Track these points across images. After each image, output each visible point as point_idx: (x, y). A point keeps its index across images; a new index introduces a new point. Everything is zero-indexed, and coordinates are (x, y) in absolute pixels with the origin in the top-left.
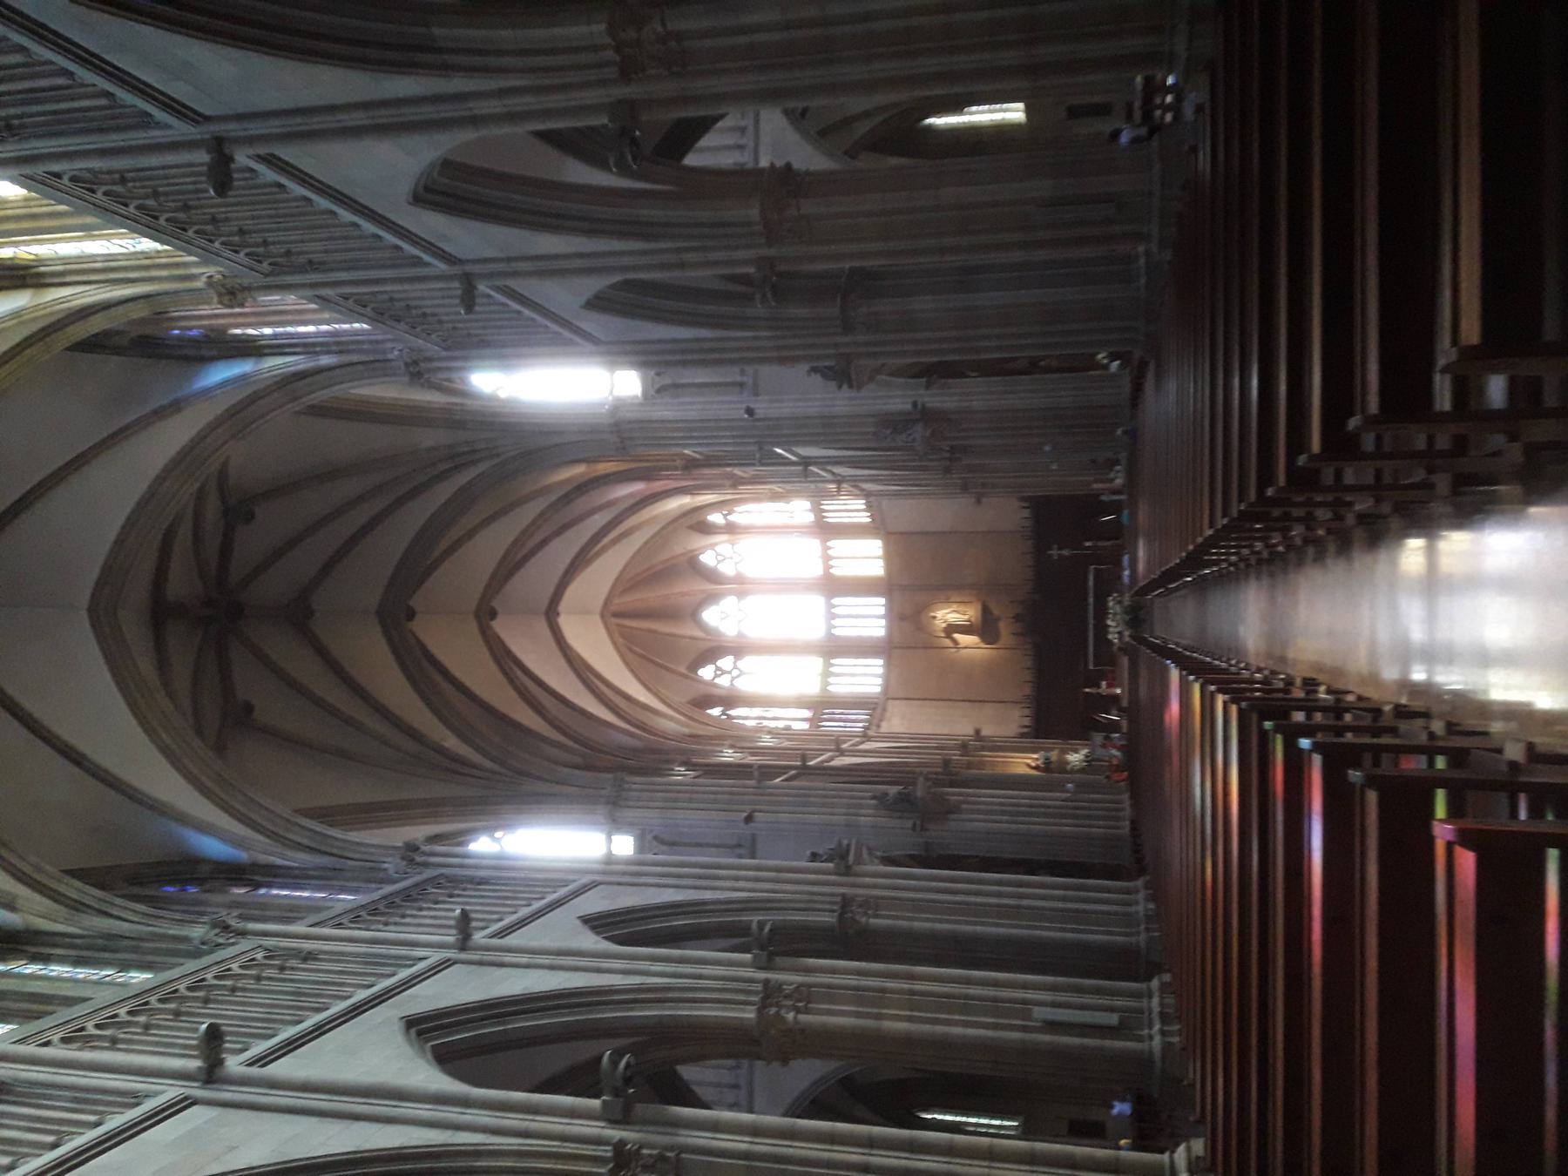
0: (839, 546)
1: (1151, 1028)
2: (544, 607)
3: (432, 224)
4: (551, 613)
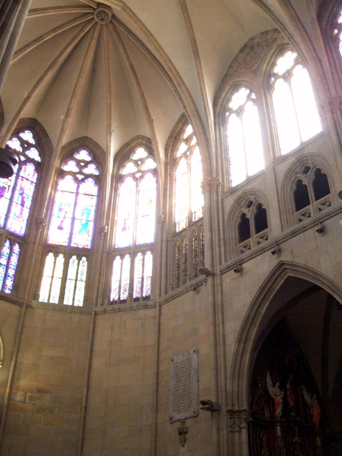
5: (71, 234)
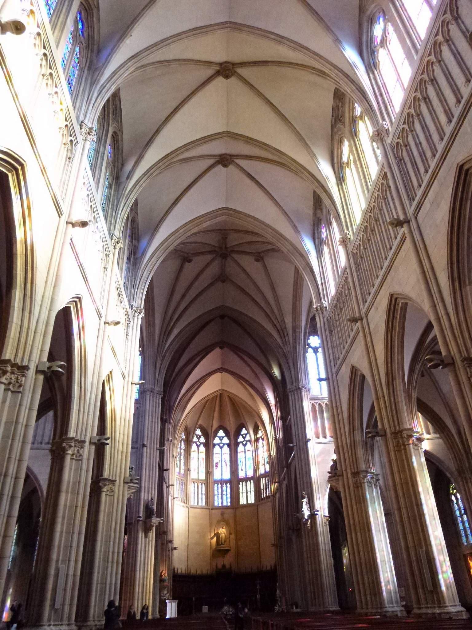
0: (251, 486)
1: (54, 625)
2: (226, 367)
3: (383, 302)
4: (221, 370)
5: (246, 471)
